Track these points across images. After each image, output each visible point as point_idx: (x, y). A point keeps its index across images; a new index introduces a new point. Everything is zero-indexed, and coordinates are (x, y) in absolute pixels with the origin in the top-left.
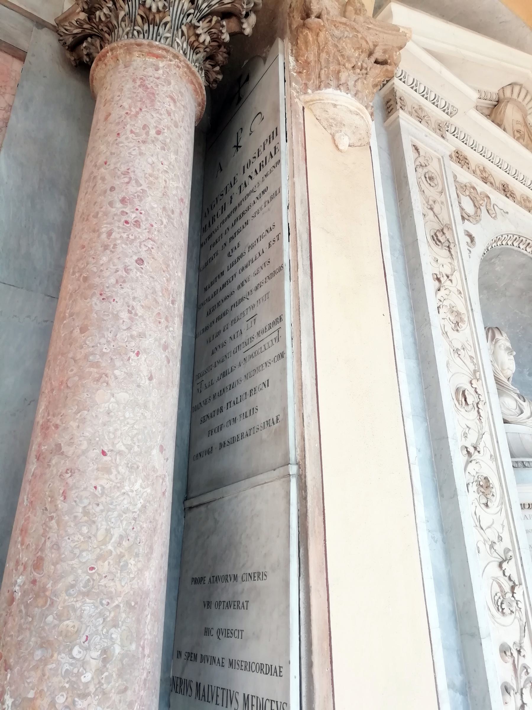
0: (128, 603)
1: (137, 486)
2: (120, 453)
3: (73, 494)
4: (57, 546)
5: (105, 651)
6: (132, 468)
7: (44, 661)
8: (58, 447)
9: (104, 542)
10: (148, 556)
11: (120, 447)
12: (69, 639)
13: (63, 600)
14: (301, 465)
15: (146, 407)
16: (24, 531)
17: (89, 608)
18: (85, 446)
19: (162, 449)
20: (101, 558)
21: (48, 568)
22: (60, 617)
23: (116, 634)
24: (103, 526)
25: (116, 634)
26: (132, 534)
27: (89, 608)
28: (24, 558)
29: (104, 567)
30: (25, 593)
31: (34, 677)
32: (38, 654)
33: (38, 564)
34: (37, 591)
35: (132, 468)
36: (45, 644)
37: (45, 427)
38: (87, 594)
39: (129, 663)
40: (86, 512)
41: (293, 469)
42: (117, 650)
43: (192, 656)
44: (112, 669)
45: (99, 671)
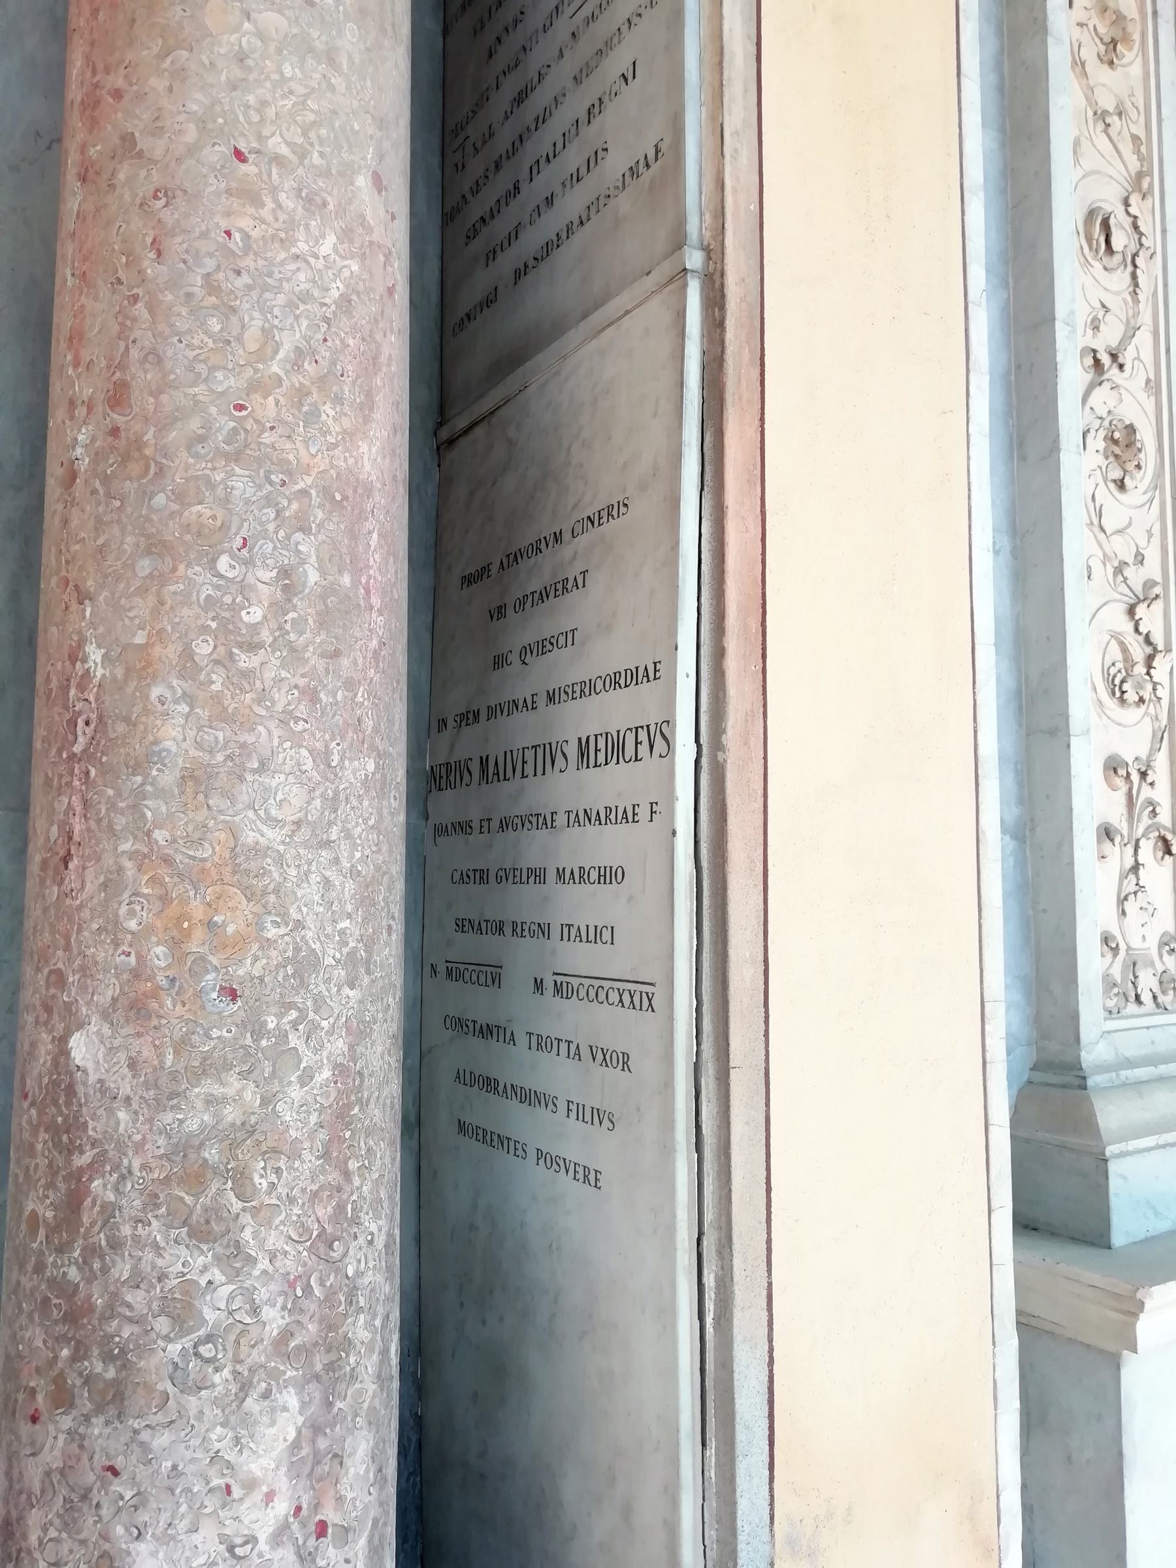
0: (326, 492)
1: (327, 246)
2: (277, 159)
3: (176, 245)
4: (155, 357)
5: (285, 573)
6: (312, 202)
7: (160, 579)
8: (128, 140)
9: (263, 355)
10: (367, 407)
11: (276, 145)
12: (209, 539)
13: (182, 466)
14: (714, 252)
15: (330, 58)
16: (76, 338)
17: (241, 484)
18: (191, 134)
19: (378, 183)
20: (254, 387)
21: (140, 400)
22: (180, 496)
23: (306, 546)
24: (256, 323)
25: (306, 546)
26: (324, 353)
27: (241, 484)
28: (85, 390)
29: (267, 408)
30: (98, 457)
31: (142, 607)
32: (145, 566)
33: (118, 396)
34: (123, 449)
35: (312, 202)
36: (155, 546)
37: (91, 103)
38: (236, 457)
39: (335, 611)
40: (212, 287)
41: (694, 259)
42: (313, 577)
43: (469, 717)
44: (303, 608)
45: (278, 608)
